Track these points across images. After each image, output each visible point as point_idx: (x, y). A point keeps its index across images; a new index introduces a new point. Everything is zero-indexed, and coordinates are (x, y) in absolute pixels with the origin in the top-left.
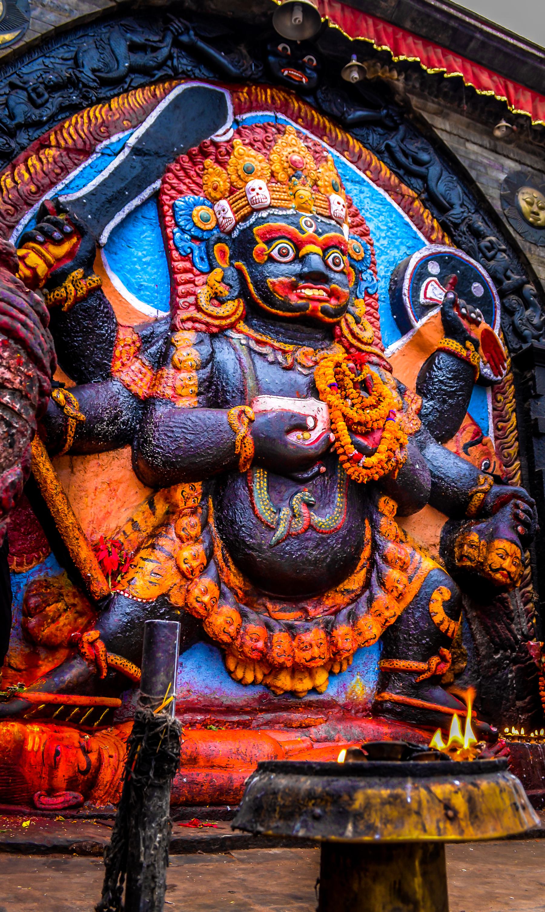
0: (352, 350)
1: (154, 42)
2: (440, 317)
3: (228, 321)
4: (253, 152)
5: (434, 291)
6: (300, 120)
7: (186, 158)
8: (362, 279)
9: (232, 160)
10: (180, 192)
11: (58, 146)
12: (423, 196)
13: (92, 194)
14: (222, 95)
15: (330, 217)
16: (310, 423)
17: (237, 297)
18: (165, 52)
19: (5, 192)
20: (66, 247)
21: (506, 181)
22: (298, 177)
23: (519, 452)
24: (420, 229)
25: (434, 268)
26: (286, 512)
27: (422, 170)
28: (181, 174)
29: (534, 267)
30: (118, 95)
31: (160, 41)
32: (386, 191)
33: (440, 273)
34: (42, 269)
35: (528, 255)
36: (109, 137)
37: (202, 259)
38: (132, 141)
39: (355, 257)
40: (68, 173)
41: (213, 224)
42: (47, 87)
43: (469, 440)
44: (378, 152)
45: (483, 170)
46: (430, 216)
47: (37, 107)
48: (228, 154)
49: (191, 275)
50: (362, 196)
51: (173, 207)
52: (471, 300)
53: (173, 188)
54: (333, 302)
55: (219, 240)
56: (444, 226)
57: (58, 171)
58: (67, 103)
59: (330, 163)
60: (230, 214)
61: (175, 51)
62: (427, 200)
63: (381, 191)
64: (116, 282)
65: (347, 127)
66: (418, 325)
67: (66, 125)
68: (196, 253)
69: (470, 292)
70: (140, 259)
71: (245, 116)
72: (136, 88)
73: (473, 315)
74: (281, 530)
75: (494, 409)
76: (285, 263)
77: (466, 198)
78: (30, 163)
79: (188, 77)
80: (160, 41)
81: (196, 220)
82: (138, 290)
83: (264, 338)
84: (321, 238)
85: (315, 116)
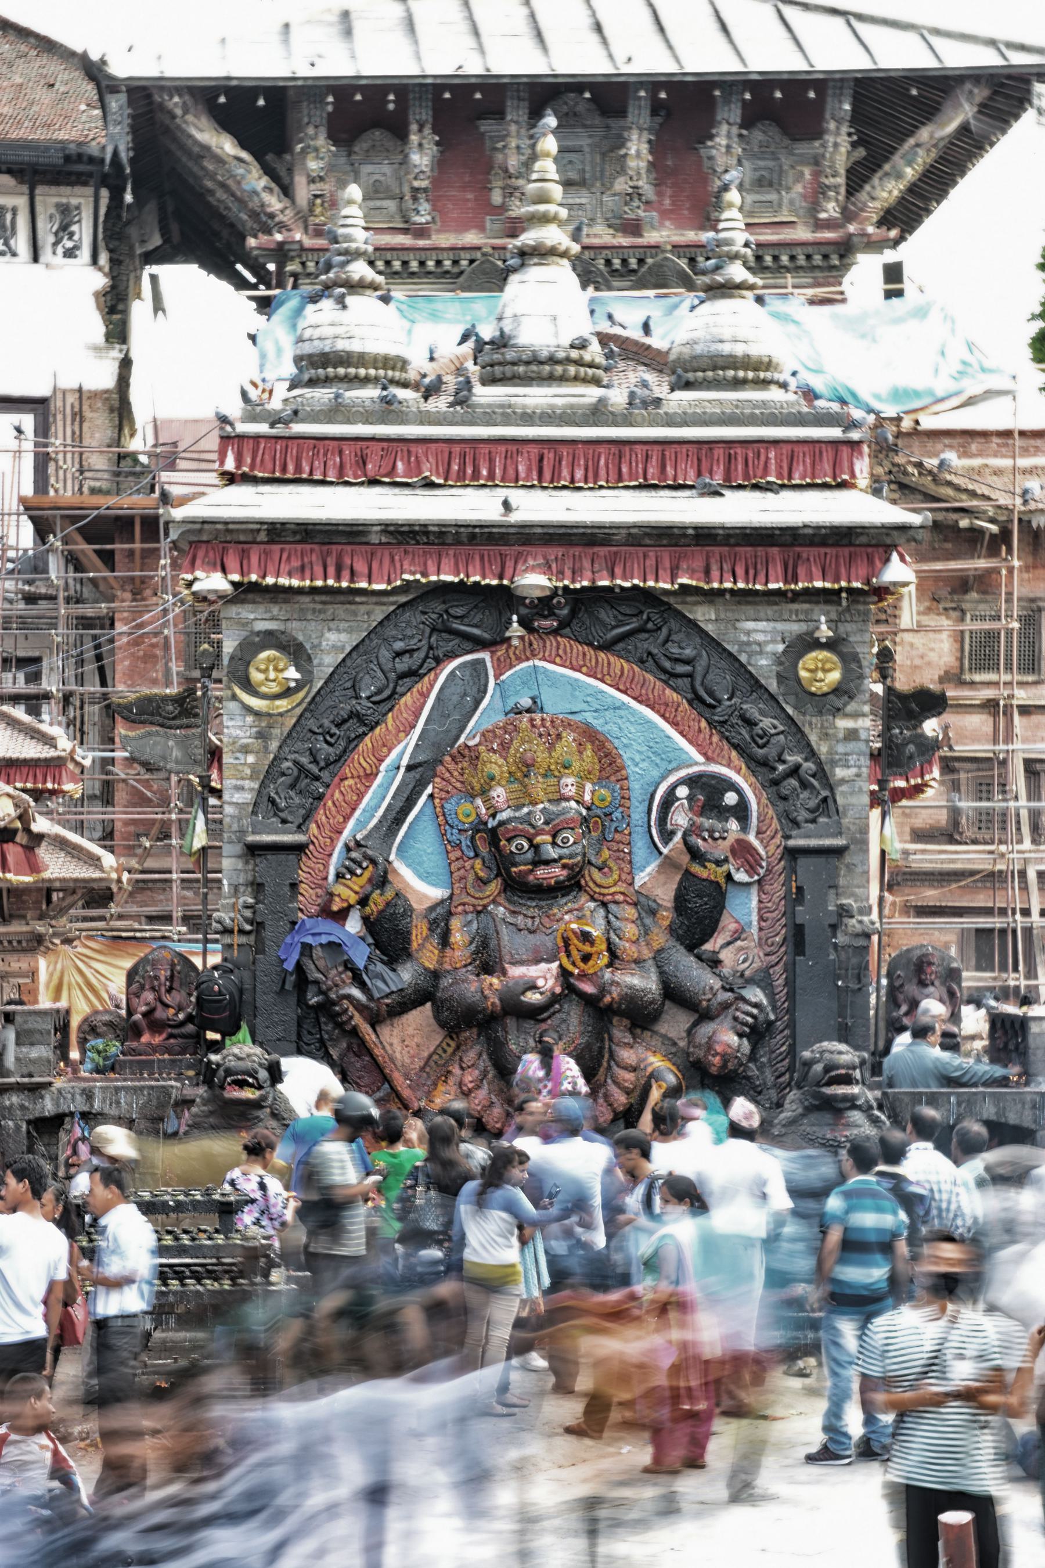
4: (495, 757)
16: (540, 983)
20: (367, 874)
21: (785, 652)
25: (682, 792)
27: (687, 668)
34: (353, 898)
38: (405, 762)
42: (338, 726)
52: (723, 812)
54: (565, 873)
55: (478, 831)
65: (607, 647)
66: (665, 851)
77: (740, 681)
79: (451, 656)
82: (424, 877)
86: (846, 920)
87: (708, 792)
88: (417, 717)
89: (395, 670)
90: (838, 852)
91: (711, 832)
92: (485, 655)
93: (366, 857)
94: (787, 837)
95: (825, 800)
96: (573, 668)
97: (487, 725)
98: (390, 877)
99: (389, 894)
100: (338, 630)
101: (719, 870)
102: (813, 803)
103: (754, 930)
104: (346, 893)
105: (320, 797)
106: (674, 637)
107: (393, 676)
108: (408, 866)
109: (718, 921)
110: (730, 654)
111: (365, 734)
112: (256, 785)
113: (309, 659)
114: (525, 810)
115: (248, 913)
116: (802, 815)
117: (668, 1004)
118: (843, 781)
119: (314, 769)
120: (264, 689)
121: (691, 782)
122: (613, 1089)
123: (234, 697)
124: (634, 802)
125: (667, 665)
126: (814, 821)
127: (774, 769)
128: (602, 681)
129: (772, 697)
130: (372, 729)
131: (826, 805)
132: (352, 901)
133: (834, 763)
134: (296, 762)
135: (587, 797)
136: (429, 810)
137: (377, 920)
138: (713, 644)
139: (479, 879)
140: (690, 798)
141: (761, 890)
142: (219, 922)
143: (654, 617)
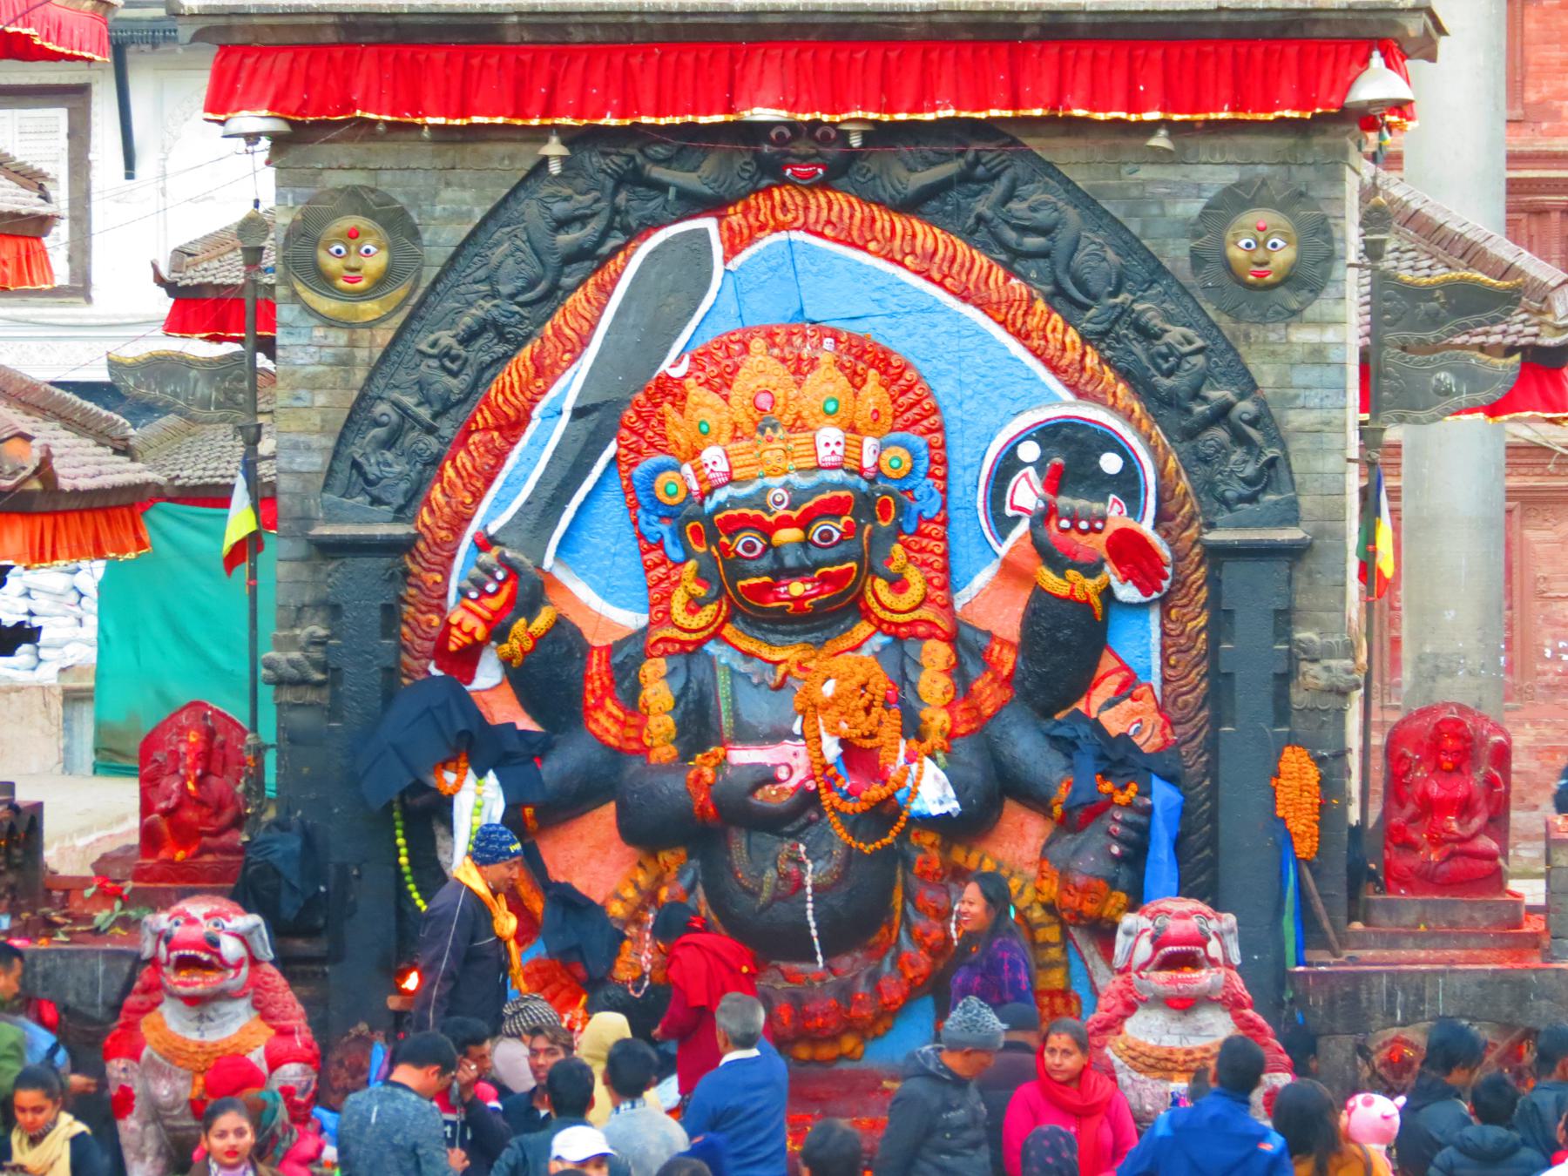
0: (885, 626)
1: (588, 207)
2: (1029, 538)
3: (705, 633)
4: (713, 399)
5: (1026, 493)
6: (828, 231)
7: (641, 397)
8: (914, 499)
9: (688, 412)
10: (639, 452)
11: (486, 429)
12: (1048, 288)
13: (528, 503)
14: (703, 234)
15: (819, 467)
16: (783, 773)
17: (715, 598)
18: (605, 215)
19: (438, 514)
21: (1203, 215)
22: (762, 431)
23: (1206, 698)
24: (1038, 356)
25: (1029, 452)
26: (771, 874)
28: (639, 425)
29: (1252, 368)
30: (550, 316)
31: (597, 201)
32: (977, 306)
33: (1042, 457)
35: (1242, 350)
36: (544, 393)
37: (674, 544)
38: (568, 405)
39: (894, 475)
40: (504, 460)
41: (683, 495)
43: (1111, 696)
44: (969, 235)
45: (1155, 210)
46: (1060, 326)
47: (454, 374)
48: (684, 398)
49: (663, 570)
50: (932, 333)
51: (630, 479)
52: (1100, 485)
53: (631, 450)
54: (827, 588)
55: (689, 519)
56: (1082, 336)
57: (492, 463)
58: (487, 359)
59: (824, 367)
60: (695, 487)
61: (621, 199)
62: (1054, 295)
63: (969, 311)
64: (582, 590)
65: (911, 206)
67: (493, 394)
68: (667, 539)
69: (1099, 469)
70: (607, 550)
71: (739, 260)
72: (574, 289)
73: (1084, 525)
74: (766, 895)
75: (1164, 634)
76: (753, 559)
78: (459, 464)
80: (597, 201)
81: (661, 495)
83: (753, 647)
84: (795, 515)
85: (857, 206)
86: (1305, 666)
87: (1071, 454)
88: (593, 327)
89: (552, 251)
90: (1294, 553)
91: (1074, 519)
92: (709, 224)
93: (503, 562)
94: (1211, 526)
95: (1272, 463)
96: (853, 244)
97: (698, 346)
98: (552, 596)
99: (542, 621)
100: (463, 186)
101: (1091, 584)
102: (1250, 470)
103: (1156, 681)
104: (466, 621)
105: (436, 461)
106: (1022, 190)
107: (553, 261)
108: (582, 575)
109: (1094, 665)
110: (1114, 220)
111: (507, 357)
112: (330, 442)
113: (415, 234)
114: (759, 483)
115: (317, 653)
116: (1233, 490)
117: (1010, 805)
118: (1300, 431)
119: (424, 413)
120: (341, 283)
121: (1048, 434)
122: (906, 945)
123: (295, 297)
124: (955, 470)
125: (1011, 236)
126: (1252, 499)
127: (1189, 411)
128: (901, 264)
129: (1185, 291)
130: (520, 346)
131: (1271, 474)
132: (479, 635)
133: (1289, 402)
134: (396, 404)
135: (868, 462)
136: (615, 486)
137: (524, 666)
138: (1086, 202)
139: (692, 598)
140: (1039, 465)
141: (1165, 614)
142: (268, 667)
143: (986, 157)
